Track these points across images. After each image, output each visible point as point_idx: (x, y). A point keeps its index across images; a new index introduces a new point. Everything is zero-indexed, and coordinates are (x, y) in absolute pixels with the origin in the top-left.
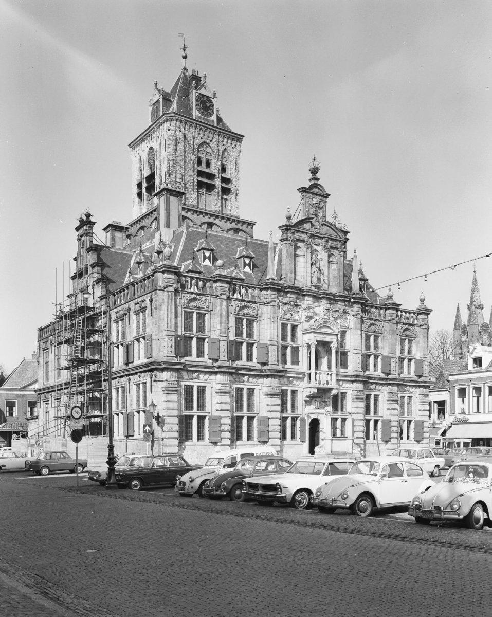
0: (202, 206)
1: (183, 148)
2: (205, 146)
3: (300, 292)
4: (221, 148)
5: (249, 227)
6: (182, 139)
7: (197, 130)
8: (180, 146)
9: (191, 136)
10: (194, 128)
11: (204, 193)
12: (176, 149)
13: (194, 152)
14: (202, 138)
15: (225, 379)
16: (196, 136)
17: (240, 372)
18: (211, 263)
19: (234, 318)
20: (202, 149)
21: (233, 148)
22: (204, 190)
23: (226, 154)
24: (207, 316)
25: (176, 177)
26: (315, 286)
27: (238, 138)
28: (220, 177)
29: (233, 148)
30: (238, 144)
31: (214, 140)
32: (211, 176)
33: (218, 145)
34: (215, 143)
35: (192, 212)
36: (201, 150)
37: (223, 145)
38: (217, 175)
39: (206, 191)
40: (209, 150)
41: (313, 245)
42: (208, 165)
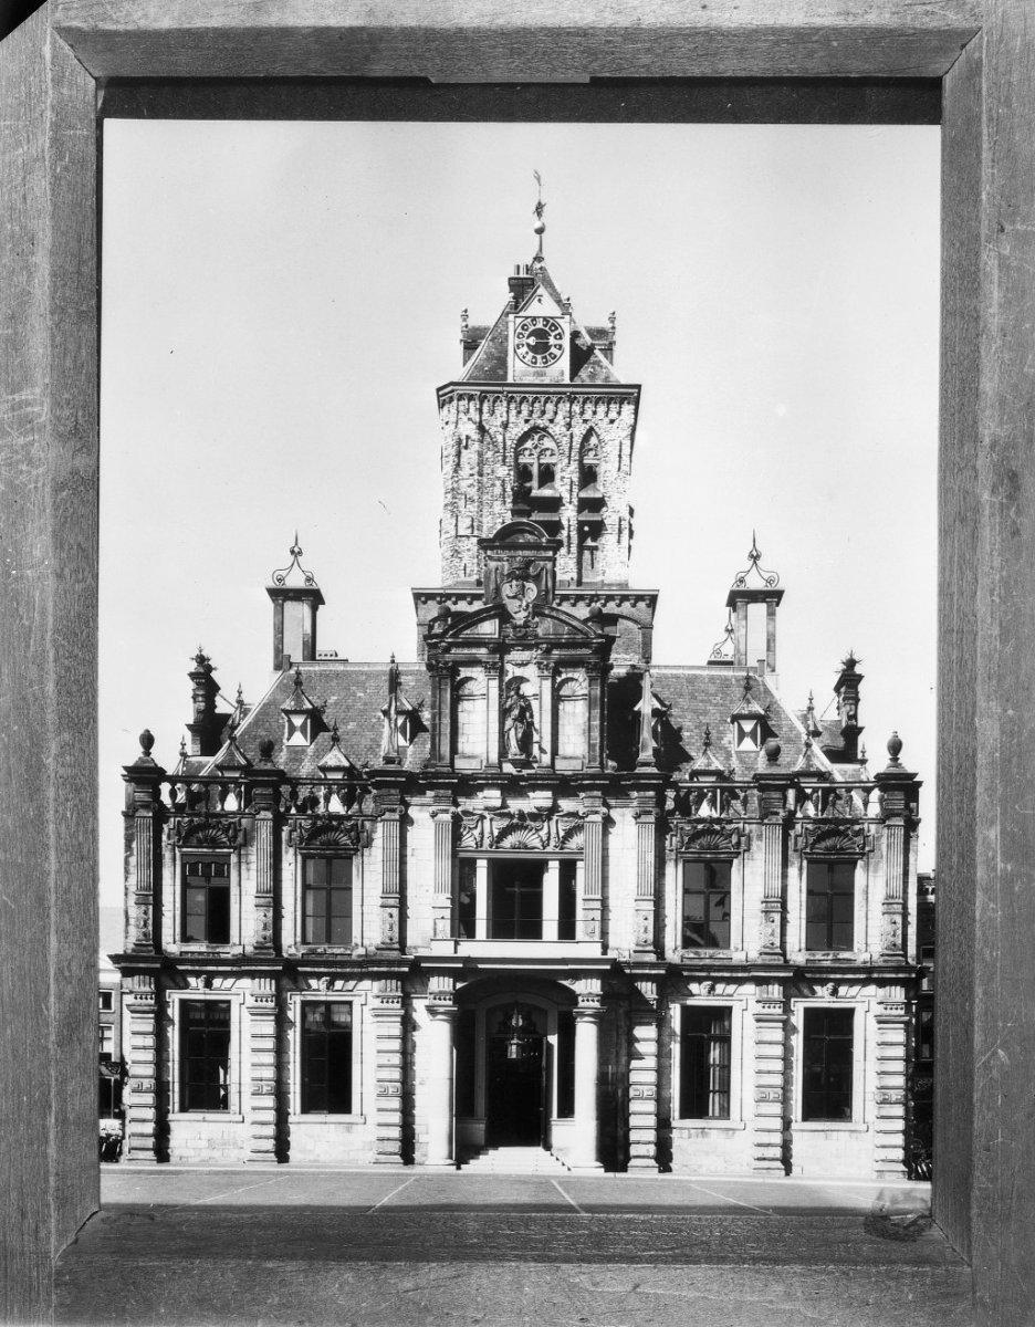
1: (475, 457)
2: (536, 437)
3: (467, 786)
4: (579, 430)
5: (642, 605)
6: (475, 436)
7: (513, 406)
8: (469, 456)
9: (499, 423)
10: (505, 404)
12: (458, 465)
13: (505, 457)
14: (527, 421)
16: (512, 419)
18: (306, 737)
19: (299, 858)
20: (529, 444)
21: (612, 421)
23: (594, 440)
24: (234, 859)
25: (456, 525)
26: (514, 763)
28: (575, 501)
29: (612, 421)
30: (628, 409)
32: (554, 504)
33: (569, 426)
34: (562, 423)
35: (454, 599)
36: (526, 449)
37: (585, 421)
38: (566, 495)
40: (548, 443)
41: (508, 667)
42: (547, 475)
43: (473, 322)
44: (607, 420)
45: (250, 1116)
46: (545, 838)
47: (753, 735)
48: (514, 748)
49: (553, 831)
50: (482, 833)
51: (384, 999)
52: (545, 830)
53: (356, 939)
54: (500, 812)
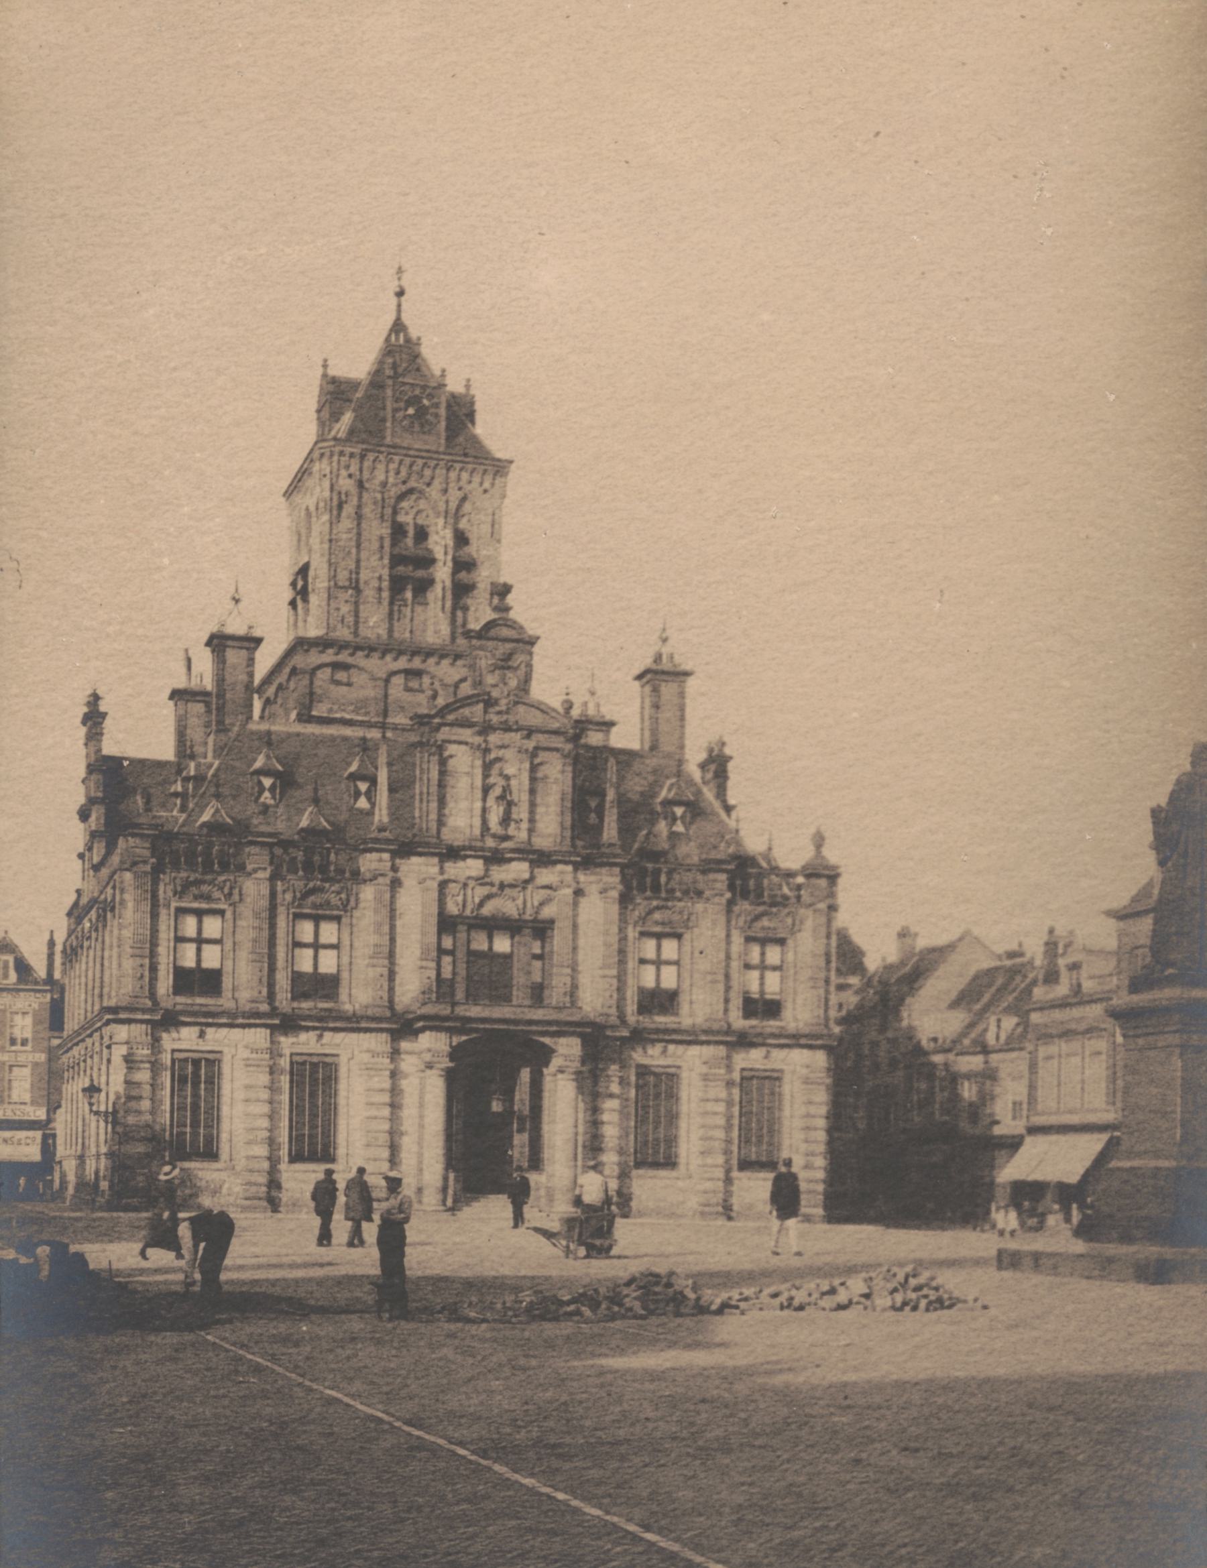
0: (402, 632)
4: (454, 495)
6: (354, 491)
8: (349, 509)
11: (409, 602)
15: (259, 1037)
16: (391, 480)
17: (303, 1023)
21: (485, 491)
22: (409, 595)
26: (494, 836)
27: (500, 468)
28: (450, 564)
29: (485, 491)
31: (436, 482)
39: (414, 597)
42: (422, 534)
43: (332, 372)
44: (481, 490)
45: (241, 1164)
46: (521, 907)
47: (683, 817)
48: (494, 819)
49: (469, 899)
50: (465, 902)
51: (374, 1054)
52: (521, 898)
53: (343, 996)
54: (481, 881)
